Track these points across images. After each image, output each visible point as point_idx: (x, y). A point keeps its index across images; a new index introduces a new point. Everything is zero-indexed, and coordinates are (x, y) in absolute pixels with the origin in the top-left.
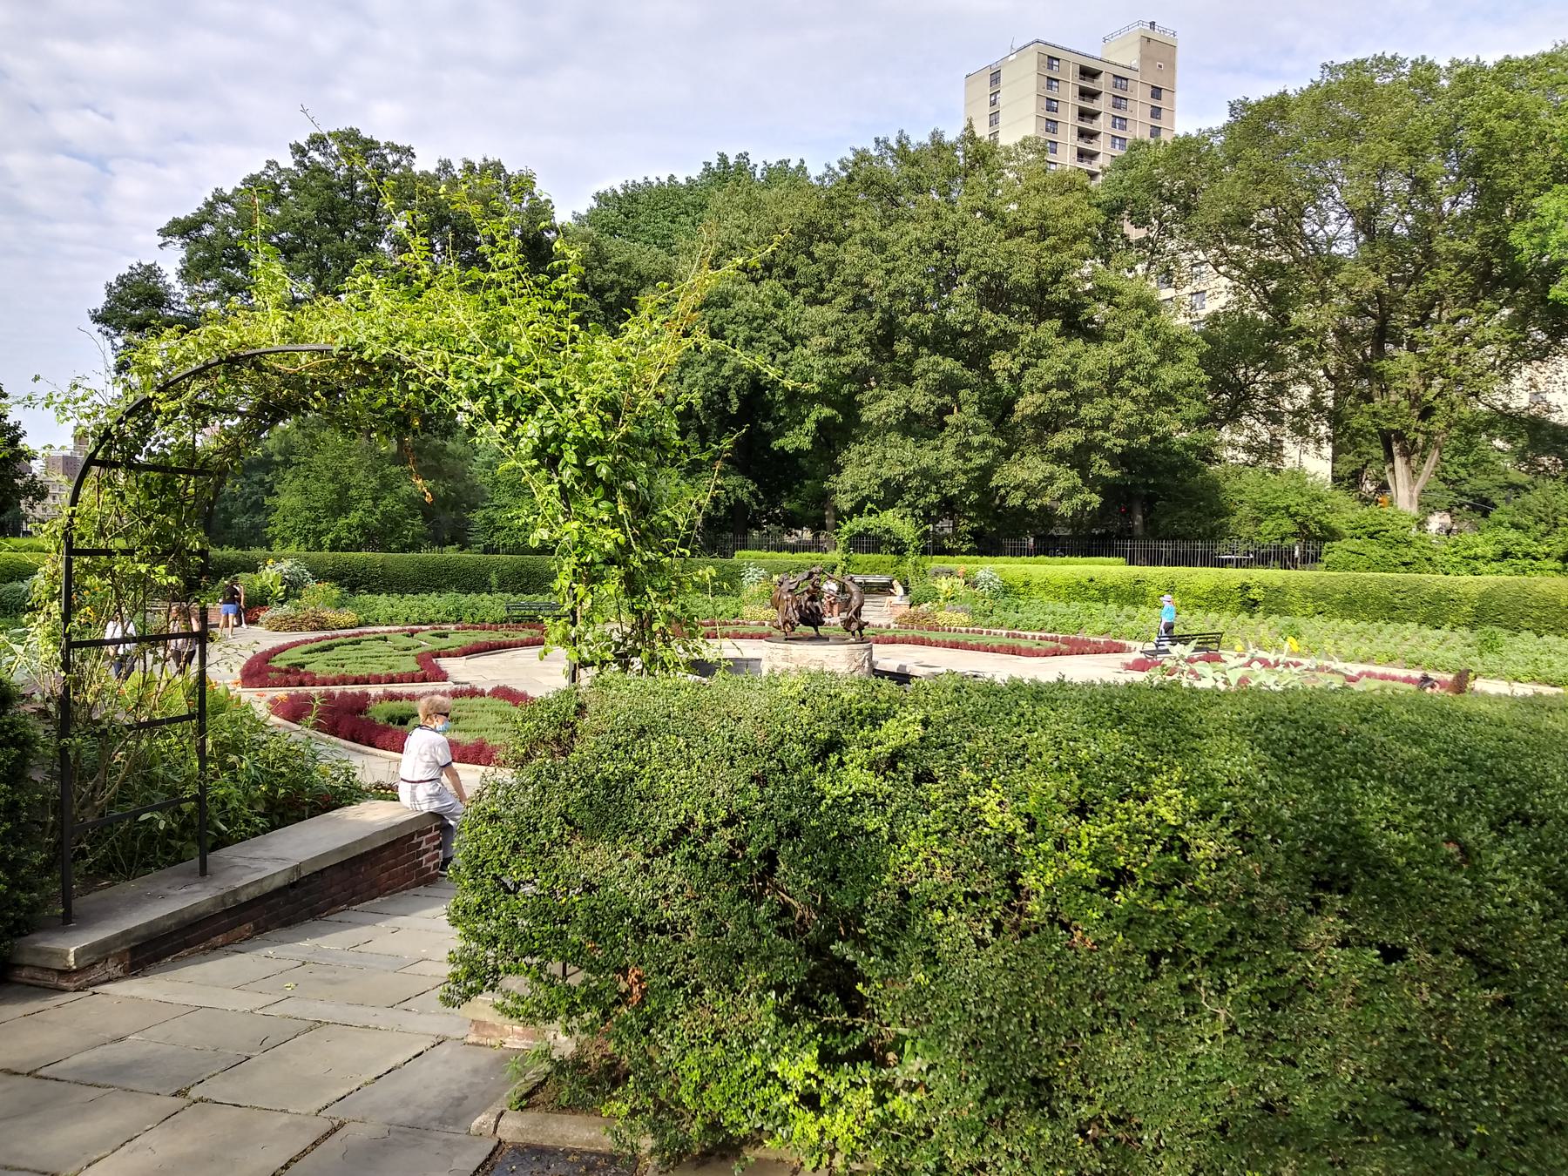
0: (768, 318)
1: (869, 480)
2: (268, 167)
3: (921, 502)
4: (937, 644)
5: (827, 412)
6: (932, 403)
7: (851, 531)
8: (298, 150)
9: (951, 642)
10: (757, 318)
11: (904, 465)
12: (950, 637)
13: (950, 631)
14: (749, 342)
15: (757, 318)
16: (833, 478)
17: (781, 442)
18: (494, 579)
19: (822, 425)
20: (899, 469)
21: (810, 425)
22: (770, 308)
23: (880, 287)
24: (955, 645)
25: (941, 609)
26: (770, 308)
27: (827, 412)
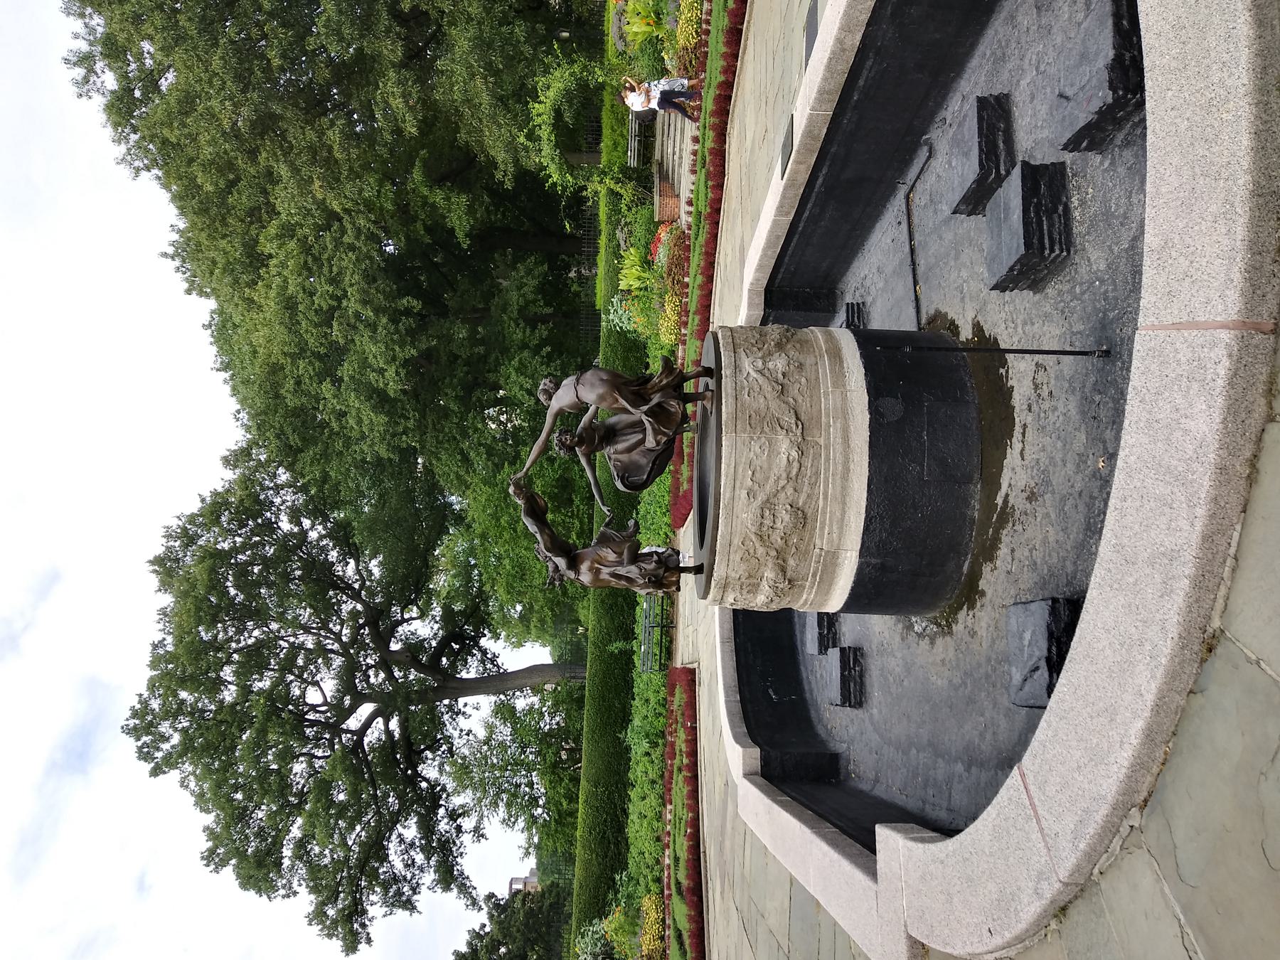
0: (306, 249)
1: (500, 126)
2: (187, 787)
3: (527, 50)
4: (730, 71)
5: (417, 174)
6: (388, 31)
7: (561, 169)
8: (156, 772)
9: (727, 44)
10: (306, 262)
11: (473, 76)
12: (717, 45)
13: (708, 22)
14: (334, 281)
15: (306, 262)
16: (499, 176)
17: (460, 235)
18: (616, 647)
19: (437, 179)
20: (479, 81)
21: (438, 197)
22: (292, 245)
23: (235, 105)
24: (735, 36)
25: (672, 35)
26: (292, 245)
27: (417, 174)
